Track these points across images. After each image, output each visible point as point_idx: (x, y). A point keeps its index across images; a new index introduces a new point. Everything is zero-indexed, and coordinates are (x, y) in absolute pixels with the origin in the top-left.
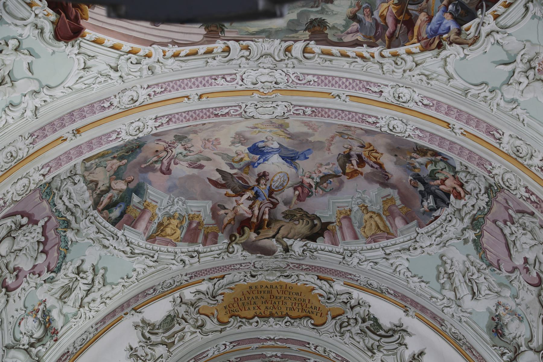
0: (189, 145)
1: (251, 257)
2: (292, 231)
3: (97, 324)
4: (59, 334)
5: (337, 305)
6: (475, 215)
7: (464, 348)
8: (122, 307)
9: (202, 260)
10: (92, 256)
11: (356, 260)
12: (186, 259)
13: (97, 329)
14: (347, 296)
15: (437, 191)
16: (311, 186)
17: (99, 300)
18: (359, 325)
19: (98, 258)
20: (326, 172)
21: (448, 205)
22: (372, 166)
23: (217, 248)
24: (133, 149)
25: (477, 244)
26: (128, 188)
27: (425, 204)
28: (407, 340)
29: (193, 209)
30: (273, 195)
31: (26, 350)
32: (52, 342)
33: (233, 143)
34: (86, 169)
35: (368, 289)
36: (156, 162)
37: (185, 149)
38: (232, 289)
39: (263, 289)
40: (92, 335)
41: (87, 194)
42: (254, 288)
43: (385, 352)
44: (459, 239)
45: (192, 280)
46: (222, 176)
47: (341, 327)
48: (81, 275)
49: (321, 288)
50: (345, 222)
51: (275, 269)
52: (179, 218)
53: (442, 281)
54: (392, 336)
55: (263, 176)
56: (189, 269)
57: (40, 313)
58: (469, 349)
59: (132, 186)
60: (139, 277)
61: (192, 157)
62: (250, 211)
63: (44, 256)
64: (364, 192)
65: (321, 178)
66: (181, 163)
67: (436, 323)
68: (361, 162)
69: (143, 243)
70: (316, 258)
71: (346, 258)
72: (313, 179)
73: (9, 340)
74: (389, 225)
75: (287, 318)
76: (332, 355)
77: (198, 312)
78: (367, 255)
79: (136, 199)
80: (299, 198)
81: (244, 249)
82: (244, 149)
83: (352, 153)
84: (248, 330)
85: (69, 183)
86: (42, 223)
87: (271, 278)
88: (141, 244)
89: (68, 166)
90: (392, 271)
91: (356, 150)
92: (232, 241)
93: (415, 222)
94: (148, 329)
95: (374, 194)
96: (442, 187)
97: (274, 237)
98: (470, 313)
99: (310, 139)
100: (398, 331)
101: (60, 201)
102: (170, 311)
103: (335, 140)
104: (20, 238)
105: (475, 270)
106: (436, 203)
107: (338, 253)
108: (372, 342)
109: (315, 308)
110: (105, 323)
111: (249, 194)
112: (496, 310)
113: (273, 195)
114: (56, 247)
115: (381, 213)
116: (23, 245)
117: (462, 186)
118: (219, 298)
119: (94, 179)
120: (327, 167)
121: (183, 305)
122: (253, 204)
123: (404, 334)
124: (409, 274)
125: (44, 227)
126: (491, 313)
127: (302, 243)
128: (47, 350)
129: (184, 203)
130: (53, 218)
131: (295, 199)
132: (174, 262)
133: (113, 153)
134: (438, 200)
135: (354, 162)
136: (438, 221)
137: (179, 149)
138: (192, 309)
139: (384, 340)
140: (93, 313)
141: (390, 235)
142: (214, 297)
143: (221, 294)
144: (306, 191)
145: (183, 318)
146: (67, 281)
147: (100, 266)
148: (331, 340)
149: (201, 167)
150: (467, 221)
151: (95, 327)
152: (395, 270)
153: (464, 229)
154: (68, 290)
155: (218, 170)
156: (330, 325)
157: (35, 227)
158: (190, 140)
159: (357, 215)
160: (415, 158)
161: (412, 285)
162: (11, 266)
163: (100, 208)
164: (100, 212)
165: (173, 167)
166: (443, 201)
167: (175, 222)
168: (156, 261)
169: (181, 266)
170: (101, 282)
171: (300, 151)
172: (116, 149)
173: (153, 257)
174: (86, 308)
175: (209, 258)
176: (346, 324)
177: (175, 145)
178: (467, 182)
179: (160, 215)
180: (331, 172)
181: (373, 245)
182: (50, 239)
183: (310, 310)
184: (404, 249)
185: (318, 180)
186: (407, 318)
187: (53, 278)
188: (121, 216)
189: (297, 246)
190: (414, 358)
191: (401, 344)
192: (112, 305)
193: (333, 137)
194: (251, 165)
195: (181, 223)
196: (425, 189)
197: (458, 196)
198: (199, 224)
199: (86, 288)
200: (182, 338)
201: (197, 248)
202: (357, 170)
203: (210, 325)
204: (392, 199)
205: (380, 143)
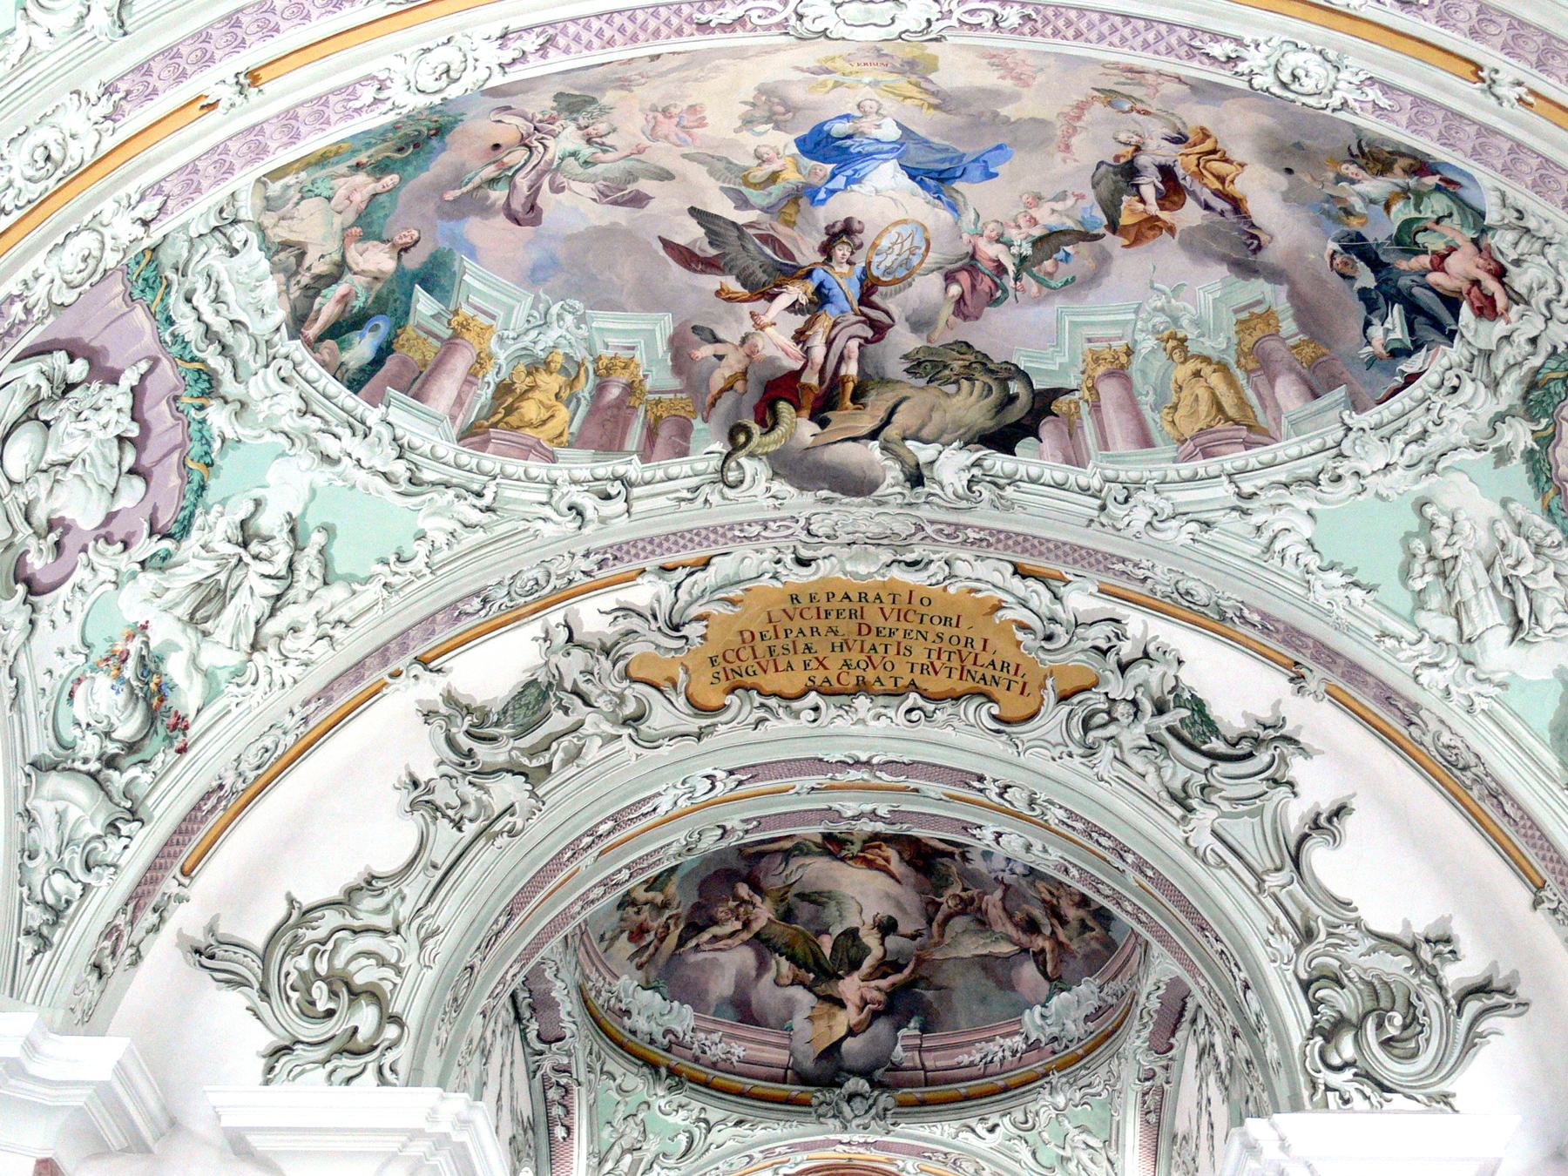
0: (602, 127)
1: (800, 502)
2: (936, 416)
3: (306, 703)
4: (192, 732)
5: (1076, 658)
6: (1537, 371)
7: (1475, 793)
8: (382, 653)
9: (637, 507)
10: (287, 485)
11: (1141, 516)
12: (588, 503)
13: (305, 720)
14: (1108, 629)
15: (1416, 291)
16: (1000, 269)
17: (311, 630)
18: (1147, 718)
19: (306, 495)
20: (1055, 222)
21: (1451, 336)
22: (1207, 207)
23: (687, 469)
24: (418, 139)
25: (1538, 463)
26: (400, 272)
27: (1376, 332)
28: (1298, 768)
29: (611, 340)
30: (875, 298)
31: (93, 776)
32: (172, 755)
33: (748, 122)
34: (270, 204)
35: (1180, 606)
36: (493, 182)
37: (589, 141)
38: (733, 602)
39: (835, 604)
40: (290, 739)
41: (271, 286)
42: (805, 601)
43: (1226, 807)
44: (1479, 448)
45: (600, 575)
46: (710, 233)
47: (1086, 726)
48: (255, 547)
49: (1024, 603)
50: (1110, 391)
51: (877, 542)
52: (563, 370)
53: (1418, 585)
54: (1250, 755)
55: (844, 232)
56: (595, 536)
57: (131, 663)
58: (1493, 795)
59: (413, 261)
60: (437, 558)
61: (610, 166)
62: (797, 350)
63: (138, 484)
64: (1176, 290)
65: (1037, 243)
66: (575, 185)
67: (1391, 717)
68: (1172, 188)
69: (448, 449)
70: (1010, 506)
71: (1111, 507)
72: (1009, 245)
73: (42, 744)
74: (1253, 399)
75: (913, 699)
76: (1055, 815)
77: (627, 675)
78: (1179, 497)
79: (424, 304)
80: (961, 307)
81: (775, 474)
82: (781, 143)
83: (1142, 160)
85: (215, 251)
86: (130, 378)
87: (863, 569)
88: (440, 452)
89: (215, 196)
90: (1257, 550)
91: (1158, 151)
92: (736, 448)
93: (1340, 393)
94: (468, 727)
95: (1207, 297)
96: (1435, 278)
97: (873, 435)
98: (1503, 685)
99: (1006, 111)
100: (1269, 740)
101: (185, 308)
102: (537, 668)
103: (1087, 117)
104: (65, 425)
105: (1526, 550)
106: (1412, 332)
107: (1084, 490)
108: (1184, 773)
109: (1005, 666)
110: (329, 701)
111: (796, 292)
113: (875, 298)
114: (175, 456)
115: (1231, 360)
116: (71, 448)
117: (1500, 273)
118: (693, 630)
119: (293, 237)
120: (1059, 206)
121: (576, 652)
122: (810, 324)
123: (1288, 749)
124: (1313, 561)
125: (137, 392)
127: (967, 457)
128: (158, 778)
129: (581, 320)
130: (165, 364)
131: (948, 310)
132: (547, 511)
133: (354, 152)
134: (1421, 319)
135: (1148, 192)
136: (1416, 390)
137: (567, 139)
138: (606, 664)
139: (1222, 767)
140: (293, 669)
141: (1255, 433)
142: (676, 628)
143: (699, 619)
144: (985, 284)
145: (576, 692)
146: (209, 567)
147: (312, 521)
148: (1053, 769)
149: (639, 200)
150: (1511, 389)
151: (300, 713)
152: (1268, 549)
153: (1501, 417)
154: (211, 598)
155: (694, 212)
156: (1053, 719)
157: (110, 390)
158: (604, 111)
159: (1150, 365)
160: (1352, 182)
161: (1321, 596)
162: (40, 515)
163: (312, 331)
164: (313, 345)
165: (546, 198)
166: (1437, 325)
167: (551, 383)
168: (489, 509)
169: (570, 524)
170: (318, 572)
171: (970, 150)
172: (368, 139)
173: (479, 495)
174: (272, 652)
175: (662, 501)
176: (1102, 718)
177: (556, 127)
178: (1517, 263)
179: (502, 356)
180: (1070, 224)
181: (1200, 465)
182: (157, 429)
183: (989, 672)
184: (1300, 481)
185: (1027, 250)
186: (1298, 699)
187: (167, 556)
188: (377, 362)
189: (952, 466)
190: (1316, 826)
191: (1276, 782)
192: (353, 645)
193: (1081, 107)
194: (802, 196)
195: (571, 384)
196: (1381, 283)
197: (1486, 309)
198: (630, 388)
199: (272, 588)
200: (575, 755)
201: (621, 470)
202: (1157, 218)
203: (664, 715)
204: (1269, 316)
205: (1237, 129)
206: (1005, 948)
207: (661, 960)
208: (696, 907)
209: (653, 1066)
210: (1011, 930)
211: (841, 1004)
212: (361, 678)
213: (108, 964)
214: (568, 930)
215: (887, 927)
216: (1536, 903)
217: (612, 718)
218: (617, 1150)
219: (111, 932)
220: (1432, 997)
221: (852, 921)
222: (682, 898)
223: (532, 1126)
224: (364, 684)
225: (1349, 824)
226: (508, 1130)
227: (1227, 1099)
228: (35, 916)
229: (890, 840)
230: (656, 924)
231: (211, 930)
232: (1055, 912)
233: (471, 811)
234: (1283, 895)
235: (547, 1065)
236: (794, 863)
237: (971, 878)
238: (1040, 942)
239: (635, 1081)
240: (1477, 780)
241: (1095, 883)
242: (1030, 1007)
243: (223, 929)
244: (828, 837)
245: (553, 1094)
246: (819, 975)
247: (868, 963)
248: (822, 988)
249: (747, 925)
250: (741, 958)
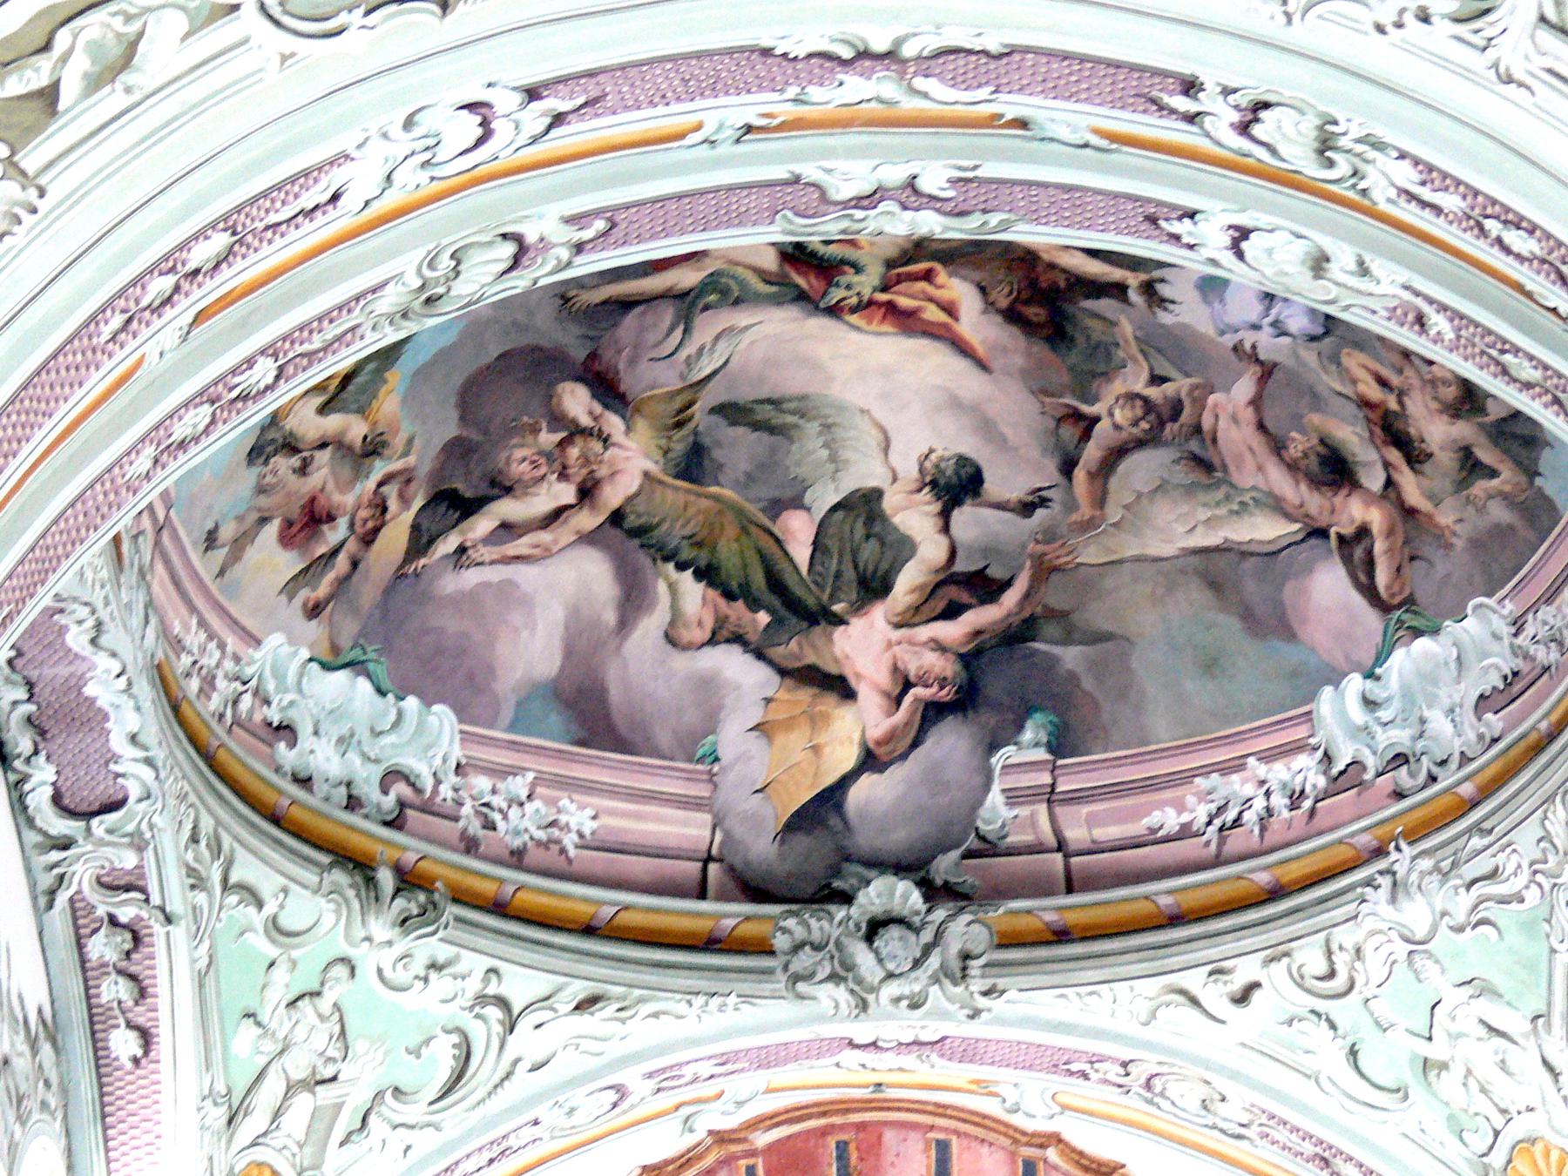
76: (1385, 179)
148: (1377, 55)
206: (1266, 529)
207: (368, 592)
208: (458, 450)
209: (360, 865)
210: (1280, 481)
211: (840, 687)
214: (121, 521)
215: (956, 486)
218: (273, 1088)
221: (865, 472)
222: (417, 429)
223: (52, 1031)
229: (955, 255)
230: (350, 498)
232: (1393, 432)
235: (82, 875)
236: (707, 326)
237: (1172, 349)
238: (1356, 511)
239: (312, 904)
241: (1495, 351)
242: (1335, 677)
244: (796, 255)
245: (102, 947)
246: (784, 609)
247: (908, 581)
248: (793, 649)
249: (587, 492)
250: (577, 578)
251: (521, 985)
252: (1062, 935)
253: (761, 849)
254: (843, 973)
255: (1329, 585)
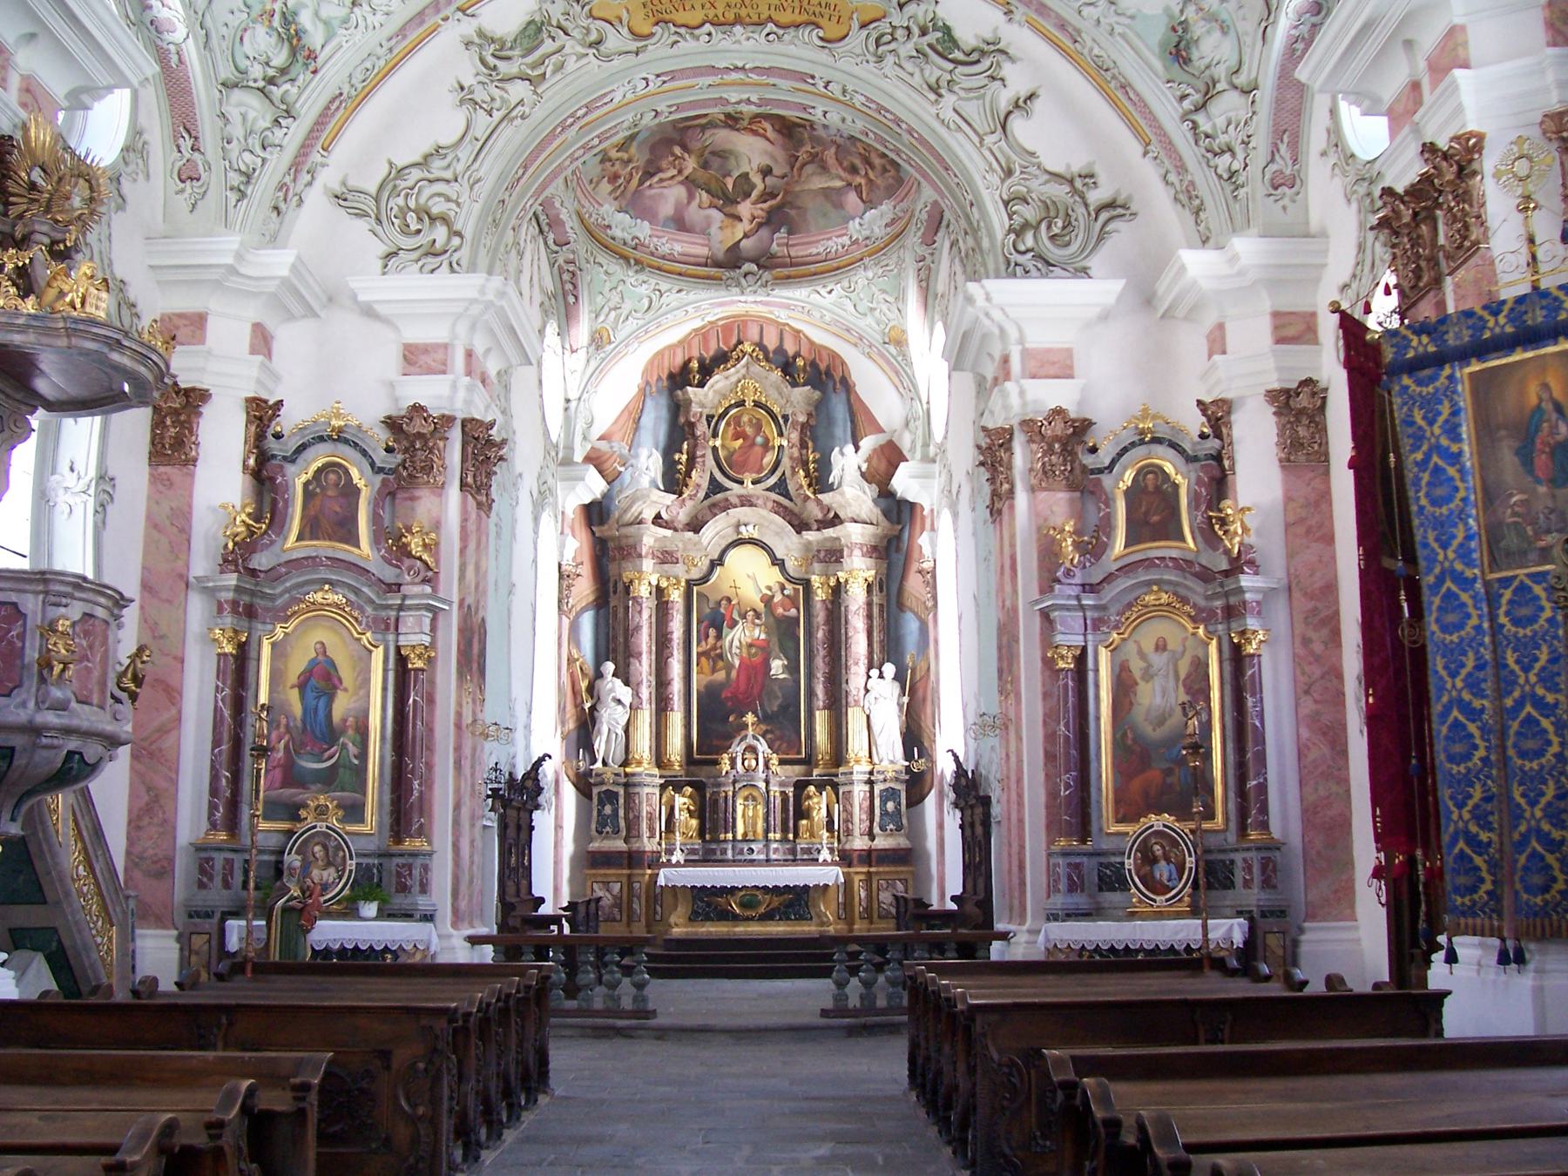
4: (320, 60)
7: (1112, 85)
13: (391, 50)
18: (915, 38)
28: (1007, 70)
31: (261, 90)
32: (309, 76)
40: (382, 62)
43: (962, 94)
54: (978, 61)
57: (277, 17)
58: (1123, 87)
67: (1064, 37)
73: (227, 73)
75: (770, 27)
76: (858, 100)
77: (591, 15)
84: (692, 51)
94: (492, 51)
98: (1132, 17)
100: (991, 51)
108: (938, 73)
110: (405, 37)
112: (1182, 12)
123: (1001, 57)
126: (1171, 17)
128: (302, 90)
138: (578, 8)
139: (961, 69)
140: (380, 17)
148: (857, 70)
151: (386, 45)
156: (857, 39)
176: (888, 38)
183: (818, 10)
190: (1017, 106)
191: (993, 78)
200: (560, 67)
207: (628, 195)
209: (626, 259)
212: (422, 22)
213: (282, 206)
216: (1145, 154)
217: (582, 43)
218: (606, 309)
219: (282, 186)
220: (1081, 210)
222: (639, 155)
224: (425, 26)
225: (1037, 105)
226: (538, 298)
227: (965, 272)
228: (235, 179)
231: (344, 184)
233: (497, 104)
234: (995, 149)
235: (561, 261)
239: (616, 268)
240: (1114, 77)
241: (883, 142)
243: (352, 183)
247: (755, 194)
248: (727, 210)
250: (677, 192)
251: (664, 286)
252: (789, 277)
253: (720, 255)
254: (738, 285)
255: (852, 197)
